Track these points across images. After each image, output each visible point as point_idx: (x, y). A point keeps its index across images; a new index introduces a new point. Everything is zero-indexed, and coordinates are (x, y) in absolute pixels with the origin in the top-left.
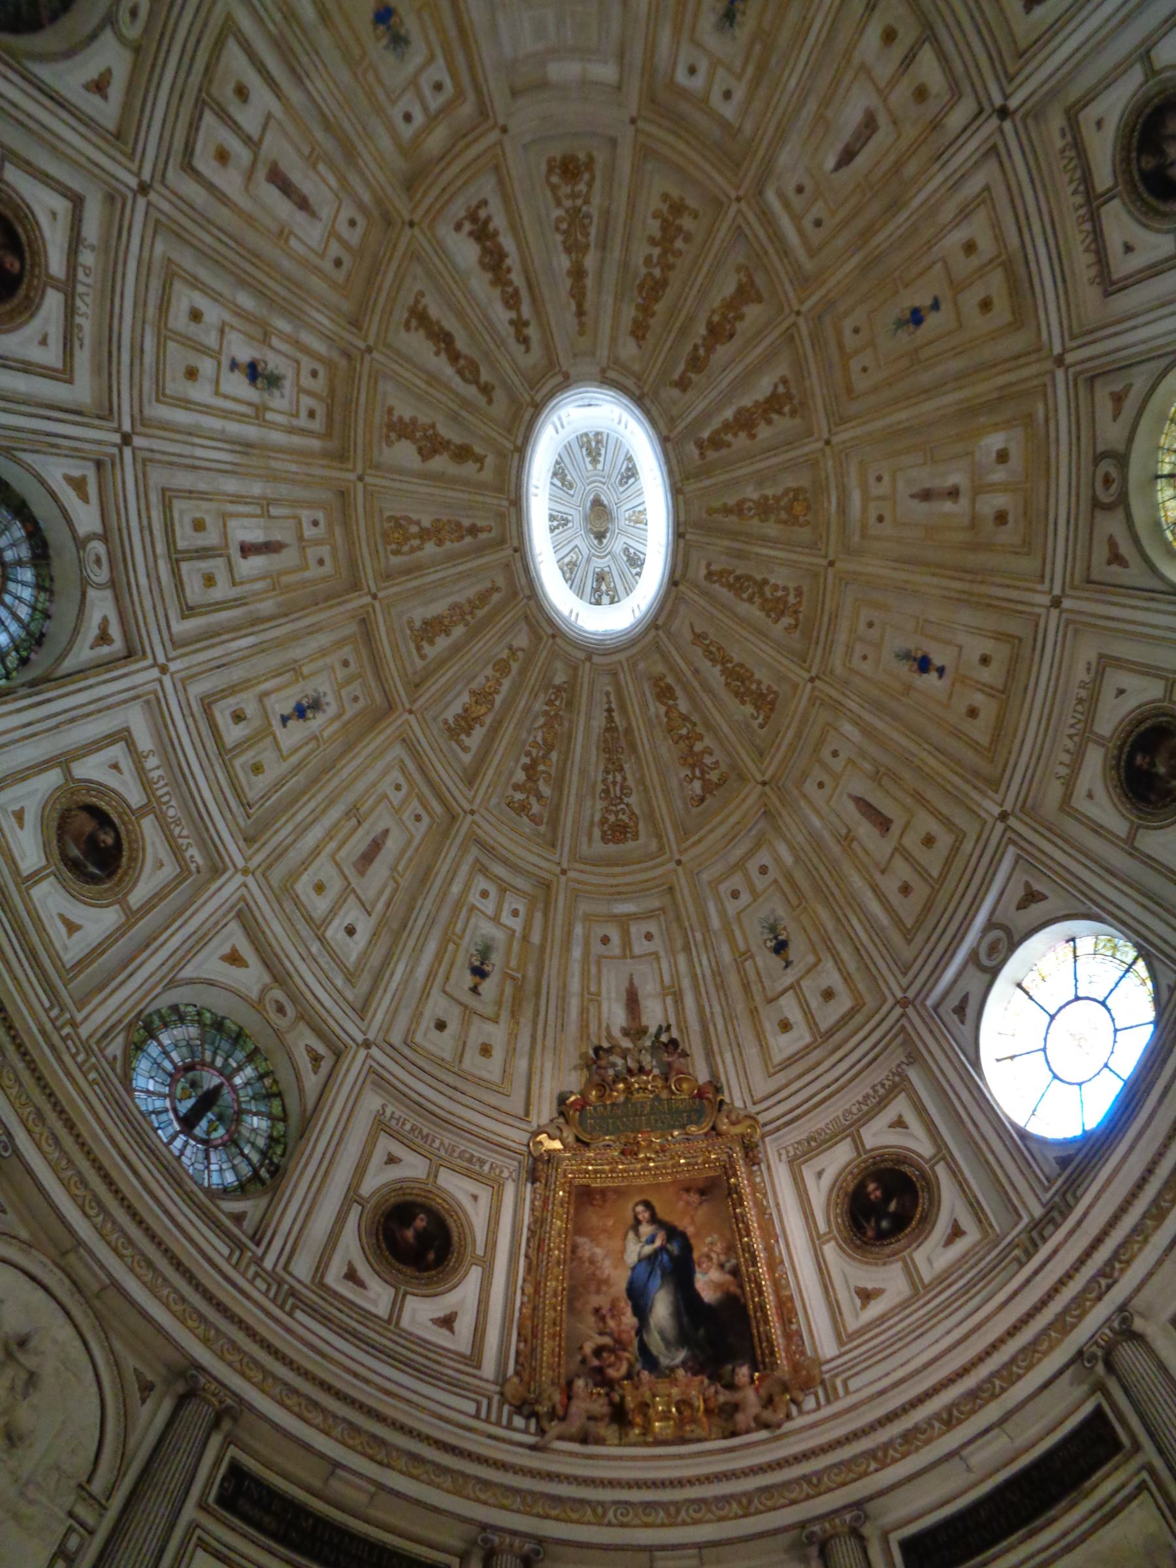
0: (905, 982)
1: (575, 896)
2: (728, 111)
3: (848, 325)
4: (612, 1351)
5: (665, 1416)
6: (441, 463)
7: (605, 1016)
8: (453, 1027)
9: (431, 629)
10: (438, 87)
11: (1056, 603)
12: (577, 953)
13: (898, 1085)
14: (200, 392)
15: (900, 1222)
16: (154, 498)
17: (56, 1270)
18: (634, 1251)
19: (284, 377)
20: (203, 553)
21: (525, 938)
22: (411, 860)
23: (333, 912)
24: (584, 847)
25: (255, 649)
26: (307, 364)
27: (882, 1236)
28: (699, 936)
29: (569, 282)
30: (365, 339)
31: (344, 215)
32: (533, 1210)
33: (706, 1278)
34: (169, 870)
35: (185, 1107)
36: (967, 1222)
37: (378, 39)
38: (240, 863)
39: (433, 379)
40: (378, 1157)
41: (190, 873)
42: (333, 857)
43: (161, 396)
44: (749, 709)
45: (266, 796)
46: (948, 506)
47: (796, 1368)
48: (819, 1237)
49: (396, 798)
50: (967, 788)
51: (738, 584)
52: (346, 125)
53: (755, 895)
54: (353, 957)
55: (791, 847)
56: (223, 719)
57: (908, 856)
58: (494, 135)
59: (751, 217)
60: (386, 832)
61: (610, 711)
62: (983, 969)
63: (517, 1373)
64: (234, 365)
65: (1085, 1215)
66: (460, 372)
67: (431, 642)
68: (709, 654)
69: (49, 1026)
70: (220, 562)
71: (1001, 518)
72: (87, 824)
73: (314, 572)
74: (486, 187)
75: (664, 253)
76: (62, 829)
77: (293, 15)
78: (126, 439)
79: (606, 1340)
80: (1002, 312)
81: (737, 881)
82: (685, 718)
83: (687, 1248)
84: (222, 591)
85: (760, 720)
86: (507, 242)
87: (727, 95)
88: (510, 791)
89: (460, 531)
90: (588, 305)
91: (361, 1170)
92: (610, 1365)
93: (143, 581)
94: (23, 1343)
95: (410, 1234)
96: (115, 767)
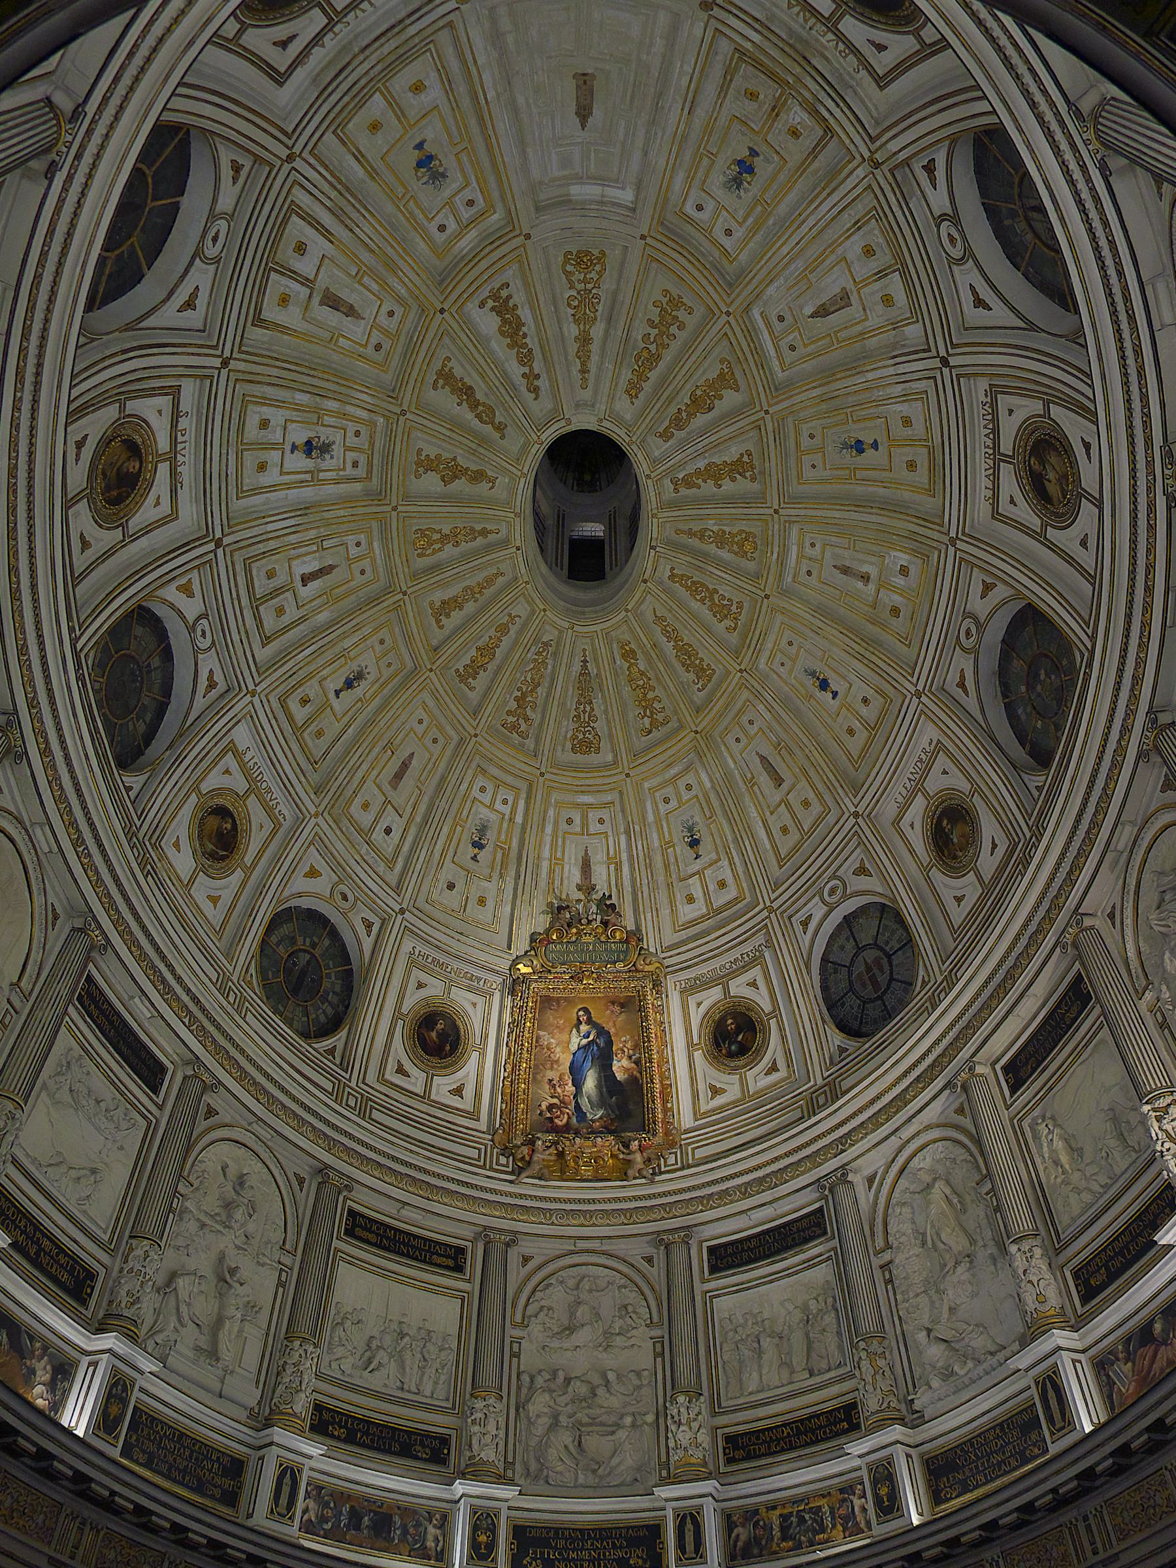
2: (727, 242)
3: (805, 429)
4: (559, 1108)
5: (586, 1164)
6: (460, 485)
7: (566, 875)
9: (445, 608)
10: (470, 203)
11: (918, 695)
12: (549, 829)
13: (755, 960)
14: (272, 476)
15: (743, 1050)
16: (239, 567)
18: (575, 1042)
19: (334, 443)
20: (277, 592)
23: (376, 821)
25: (313, 656)
26: (352, 427)
27: (731, 1055)
28: (637, 828)
29: (576, 346)
30: (401, 405)
31: (385, 309)
36: (781, 1064)
37: (419, 179)
38: (313, 810)
39: (457, 425)
41: (281, 825)
43: (241, 493)
44: (692, 676)
45: (326, 753)
46: (860, 584)
47: (667, 1133)
48: (693, 1045)
49: (420, 729)
50: (837, 785)
51: (695, 588)
52: (389, 250)
55: (711, 781)
56: (293, 705)
57: (789, 807)
58: (521, 239)
59: (737, 329)
61: (585, 661)
62: (823, 901)
63: (501, 1124)
64: (294, 448)
65: (839, 1108)
66: (478, 416)
67: (448, 616)
68: (665, 632)
70: (289, 595)
71: (895, 611)
72: (213, 822)
73: (359, 579)
74: (510, 274)
75: (661, 334)
76: (200, 837)
77: (348, 189)
78: (219, 543)
79: (555, 1101)
80: (922, 476)
81: (669, 791)
82: (642, 673)
83: (610, 1043)
84: (291, 614)
85: (699, 686)
86: (525, 314)
87: (729, 232)
88: (505, 717)
89: (473, 534)
90: (593, 367)
92: (558, 1117)
93: (236, 638)
94: (242, 1184)
95: (434, 1034)
96: (227, 772)
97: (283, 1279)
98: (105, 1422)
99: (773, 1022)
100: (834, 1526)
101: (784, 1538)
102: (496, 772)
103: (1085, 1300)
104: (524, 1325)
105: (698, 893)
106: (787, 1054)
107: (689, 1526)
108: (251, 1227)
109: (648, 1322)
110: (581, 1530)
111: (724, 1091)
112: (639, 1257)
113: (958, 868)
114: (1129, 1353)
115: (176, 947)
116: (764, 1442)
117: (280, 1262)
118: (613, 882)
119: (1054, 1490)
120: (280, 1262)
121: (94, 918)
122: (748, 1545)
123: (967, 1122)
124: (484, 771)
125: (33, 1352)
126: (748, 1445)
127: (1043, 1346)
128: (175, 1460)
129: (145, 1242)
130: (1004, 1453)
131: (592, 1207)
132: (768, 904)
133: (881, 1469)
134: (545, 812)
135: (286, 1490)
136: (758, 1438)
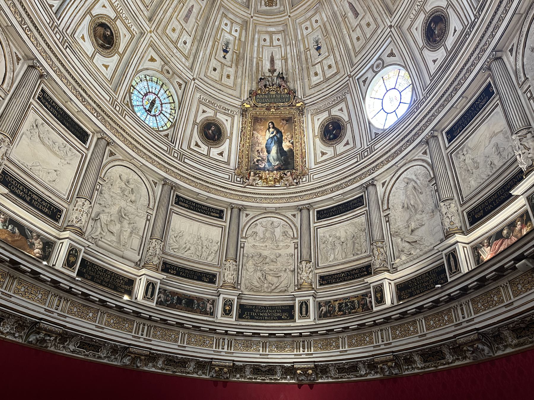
0: (351, 70)
1: (255, 26)
7: (264, 65)
8: (219, 69)
12: (256, 44)
18: (268, 135)
21: (239, 39)
22: (202, 15)
24: (259, 7)
27: (330, 139)
28: (294, 42)
32: (242, 124)
33: (285, 144)
34: (128, 36)
35: (147, 108)
36: (351, 142)
38: (149, 29)
40: (201, 111)
41: (134, 36)
42: (176, 18)
48: (315, 136)
50: (383, 12)
53: (313, 29)
54: (187, 52)
60: (193, 6)
63: (238, 167)
69: (113, 109)
72: (101, 30)
76: (95, 36)
79: (260, 158)
81: (308, 24)
91: (196, 116)
92: (261, 164)
96: (104, 6)
97: (149, 218)
98: (69, 264)
99: (349, 126)
100: (359, 307)
101: (339, 311)
102: (231, 16)
103: (471, 224)
104: (246, 238)
105: (319, 71)
106: (354, 138)
107: (304, 306)
108: (133, 198)
109: (293, 237)
110: (265, 306)
111: (326, 153)
112: (290, 215)
113: (436, 46)
114: (489, 243)
115: (85, 81)
116: (334, 278)
117: (147, 212)
118: (284, 68)
119: (449, 295)
120: (147, 212)
121: (38, 61)
122: (326, 312)
123: (427, 158)
124: (226, 16)
125: (32, 237)
126: (328, 279)
127: (452, 241)
128: (104, 279)
129: (83, 199)
130: (429, 282)
131: (273, 197)
132: (349, 73)
133: (378, 288)
134: (254, 35)
135: (150, 290)
136: (332, 277)
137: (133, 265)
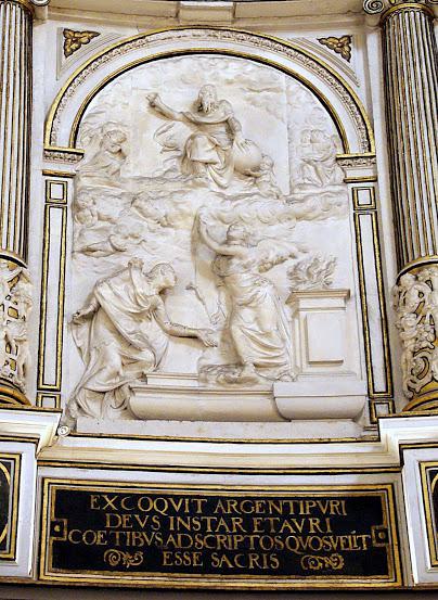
17: (181, 33)
94: (200, 108)
108: (244, 155)
117: (346, 182)
128: (212, 541)
137: (348, 429)
